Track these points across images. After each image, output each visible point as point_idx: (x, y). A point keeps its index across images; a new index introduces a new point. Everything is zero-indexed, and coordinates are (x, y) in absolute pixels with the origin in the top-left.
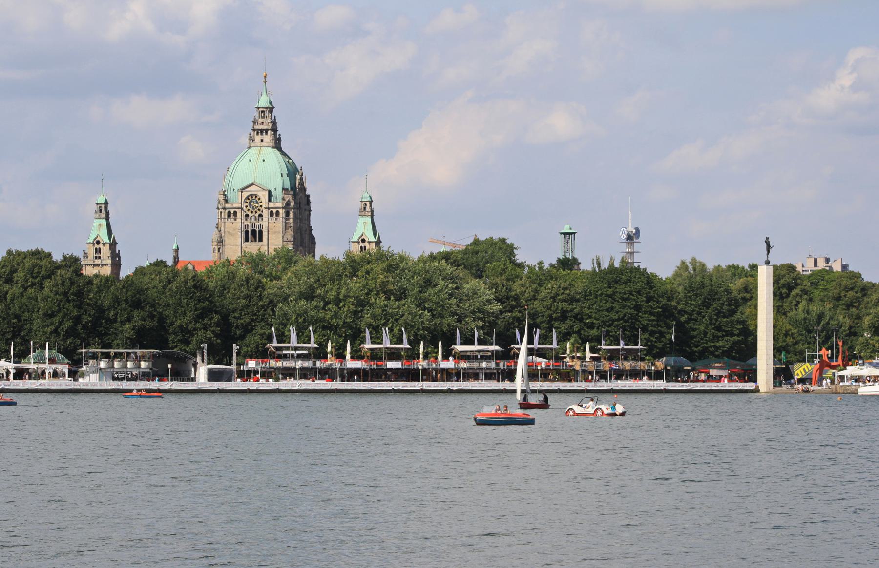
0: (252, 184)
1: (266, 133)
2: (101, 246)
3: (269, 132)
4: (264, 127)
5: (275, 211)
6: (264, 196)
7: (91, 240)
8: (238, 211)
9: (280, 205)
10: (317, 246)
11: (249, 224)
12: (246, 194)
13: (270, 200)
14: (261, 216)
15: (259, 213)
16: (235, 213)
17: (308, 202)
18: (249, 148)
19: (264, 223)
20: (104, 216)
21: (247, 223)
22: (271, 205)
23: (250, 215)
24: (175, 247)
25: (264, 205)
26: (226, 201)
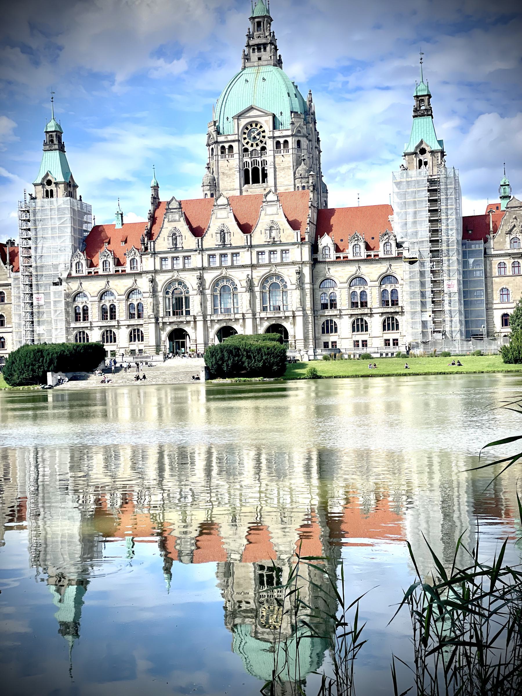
0: (251, 108)
1: (265, 49)
2: (53, 187)
3: (268, 48)
4: (264, 41)
5: (282, 140)
6: (267, 123)
7: (39, 181)
8: (235, 145)
9: (289, 133)
10: (329, 195)
11: (249, 161)
12: (244, 122)
13: (274, 128)
14: (263, 149)
15: (261, 145)
16: (231, 147)
17: (318, 140)
18: (244, 68)
19: (269, 157)
20: (57, 147)
21: (247, 159)
22: (277, 133)
23: (250, 149)
24: (153, 184)
25: (268, 134)
26: (218, 133)
